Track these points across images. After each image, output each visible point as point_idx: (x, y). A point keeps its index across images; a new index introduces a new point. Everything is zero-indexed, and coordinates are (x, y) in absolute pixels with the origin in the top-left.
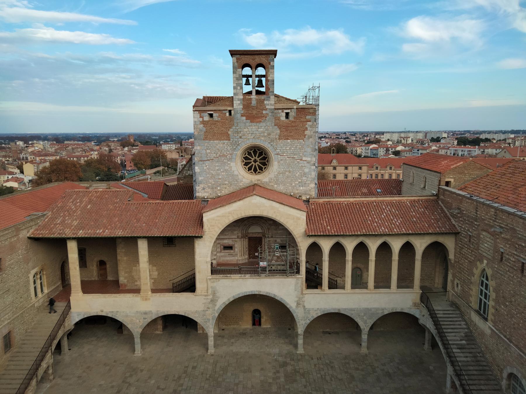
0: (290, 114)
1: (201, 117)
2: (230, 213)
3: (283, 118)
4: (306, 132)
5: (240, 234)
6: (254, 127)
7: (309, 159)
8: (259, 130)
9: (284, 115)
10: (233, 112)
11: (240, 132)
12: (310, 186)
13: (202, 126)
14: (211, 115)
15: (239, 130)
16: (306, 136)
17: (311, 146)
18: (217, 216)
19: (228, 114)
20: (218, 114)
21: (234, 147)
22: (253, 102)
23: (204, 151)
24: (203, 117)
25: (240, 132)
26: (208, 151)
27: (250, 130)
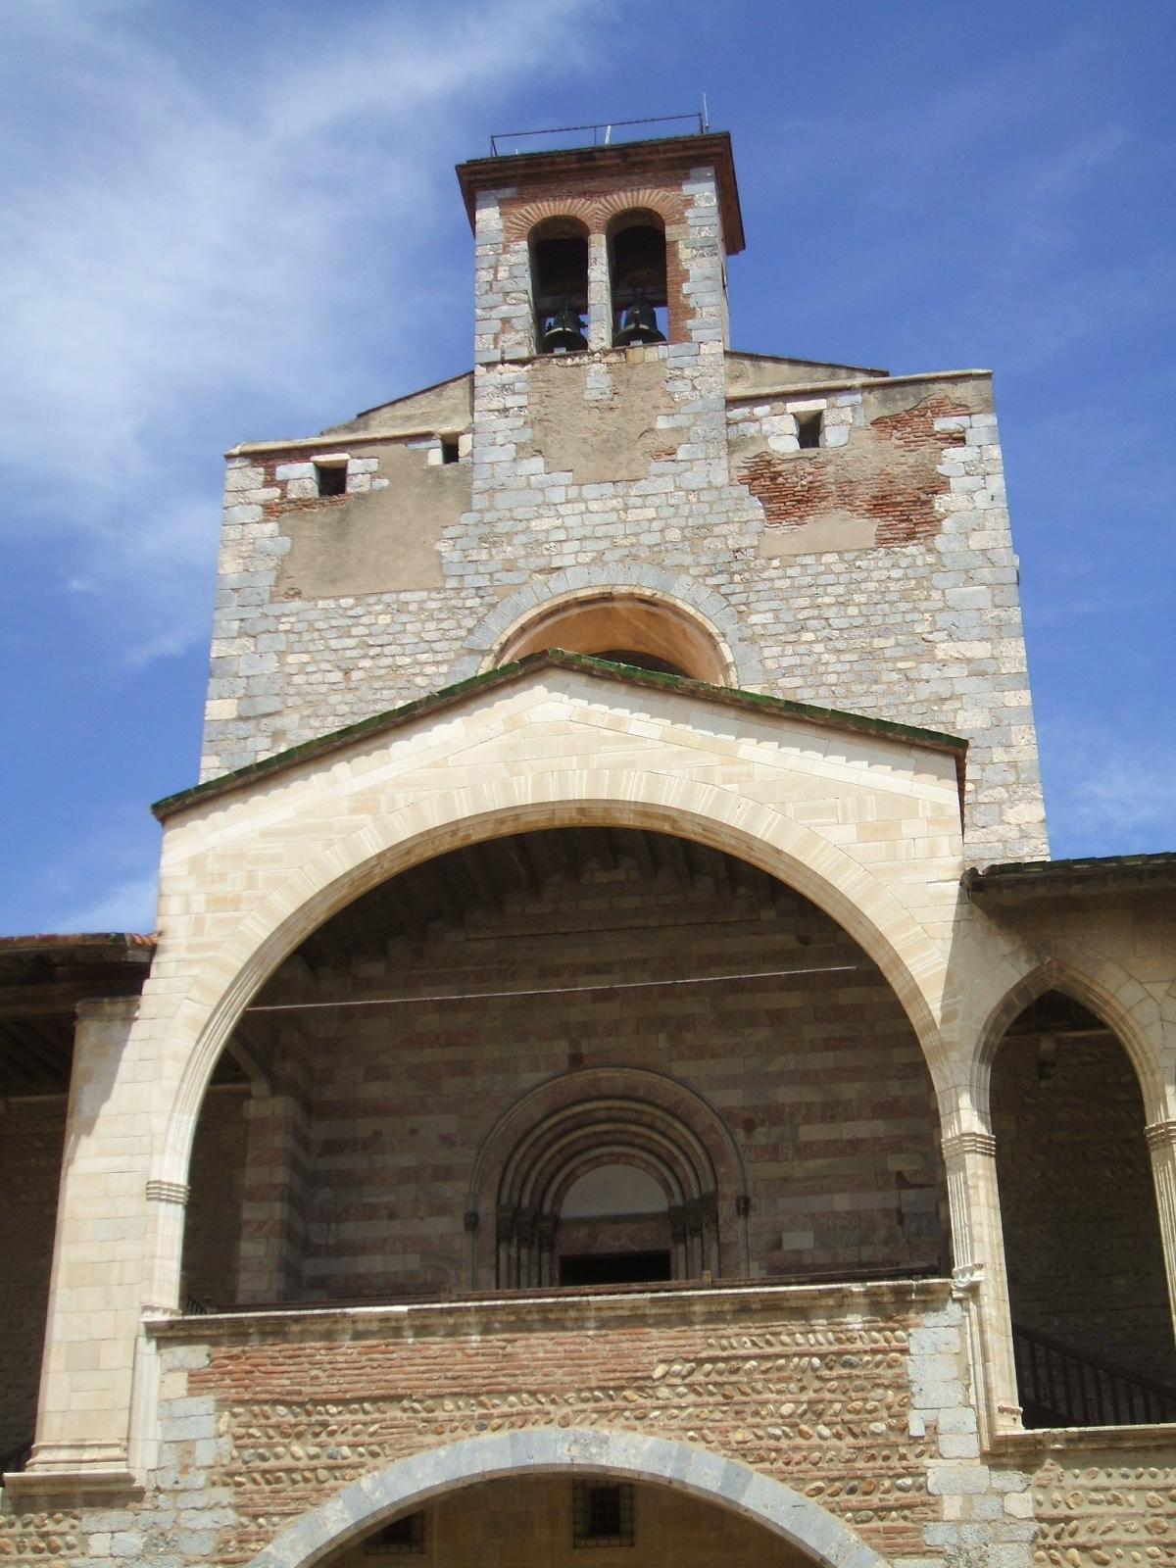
0: (827, 420)
1: (270, 482)
2: (363, 803)
3: (784, 442)
4: (940, 503)
5: (487, 1207)
6: (594, 506)
7: (980, 650)
8: (633, 515)
9: (792, 427)
10: (465, 444)
11: (509, 536)
12: (1010, 815)
13: (271, 527)
14: (332, 480)
15: (501, 528)
16: (947, 524)
17: (986, 574)
18: (266, 834)
19: (436, 457)
20: (373, 465)
21: (470, 623)
22: (591, 383)
23: (271, 665)
24: (283, 485)
25: (509, 536)
26: (291, 659)
27: (569, 522)
